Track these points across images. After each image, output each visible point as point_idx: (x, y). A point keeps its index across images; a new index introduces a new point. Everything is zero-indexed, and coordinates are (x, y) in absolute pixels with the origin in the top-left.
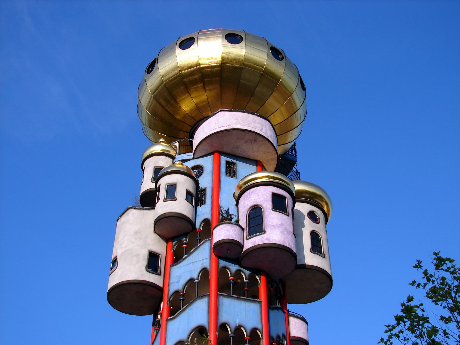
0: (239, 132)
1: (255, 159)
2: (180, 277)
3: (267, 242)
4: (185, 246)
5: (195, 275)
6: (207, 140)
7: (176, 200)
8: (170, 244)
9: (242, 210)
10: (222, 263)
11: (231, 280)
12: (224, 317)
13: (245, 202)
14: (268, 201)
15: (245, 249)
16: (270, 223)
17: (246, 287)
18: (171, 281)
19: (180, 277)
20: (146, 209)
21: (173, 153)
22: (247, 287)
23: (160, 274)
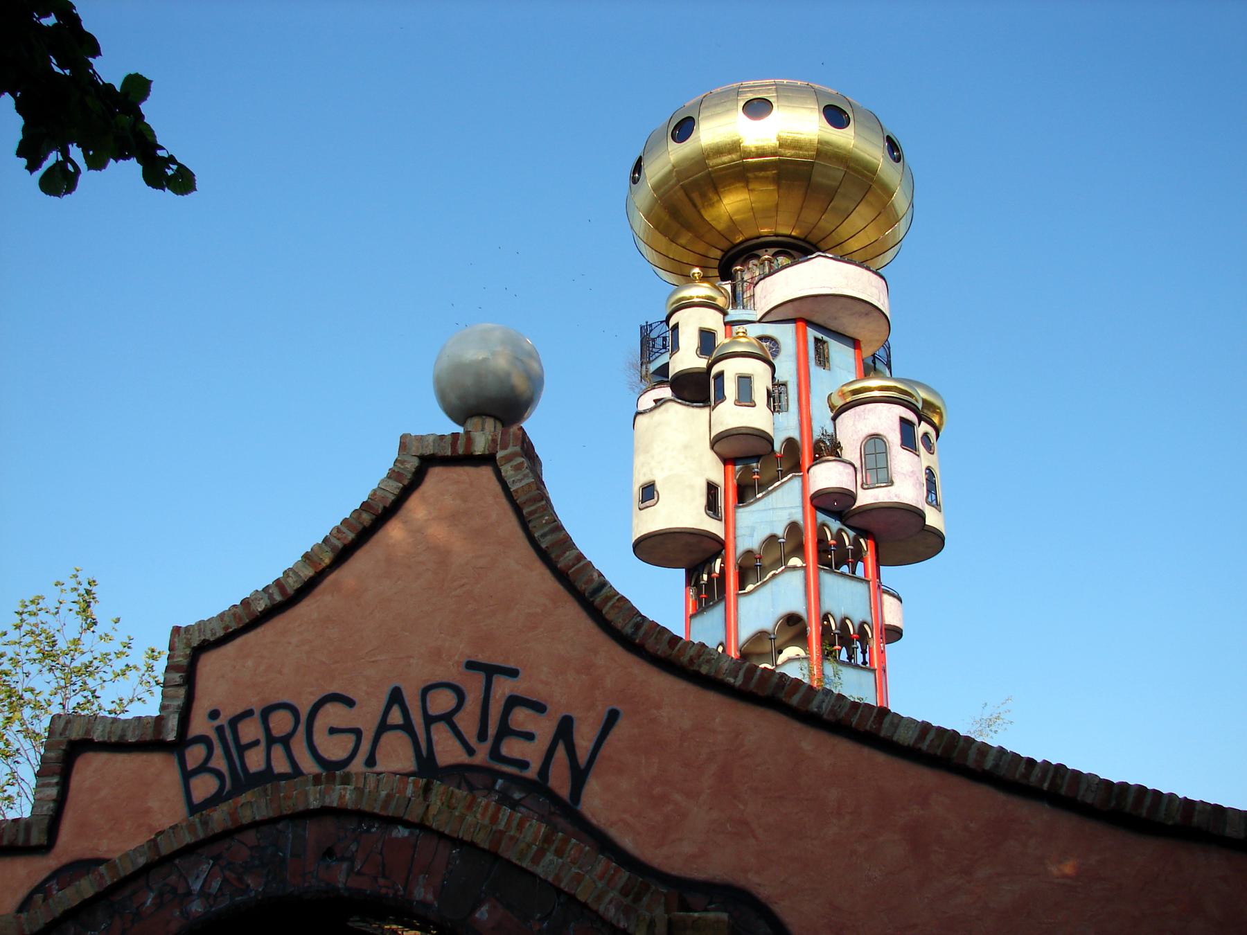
0: (849, 301)
1: (853, 336)
2: (753, 529)
3: (896, 500)
4: (756, 476)
5: (780, 531)
6: (796, 303)
7: (754, 406)
8: (730, 467)
9: (850, 435)
10: (821, 517)
11: (831, 545)
12: (827, 605)
13: (856, 423)
14: (895, 430)
15: (858, 504)
16: (899, 469)
17: (850, 557)
18: (739, 532)
19: (753, 529)
20: (697, 407)
21: (721, 301)
22: (852, 558)
23: (721, 520)
